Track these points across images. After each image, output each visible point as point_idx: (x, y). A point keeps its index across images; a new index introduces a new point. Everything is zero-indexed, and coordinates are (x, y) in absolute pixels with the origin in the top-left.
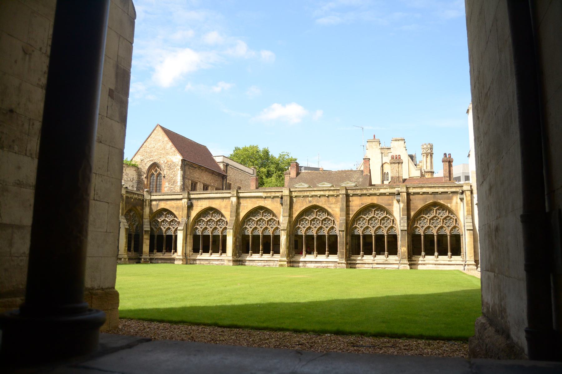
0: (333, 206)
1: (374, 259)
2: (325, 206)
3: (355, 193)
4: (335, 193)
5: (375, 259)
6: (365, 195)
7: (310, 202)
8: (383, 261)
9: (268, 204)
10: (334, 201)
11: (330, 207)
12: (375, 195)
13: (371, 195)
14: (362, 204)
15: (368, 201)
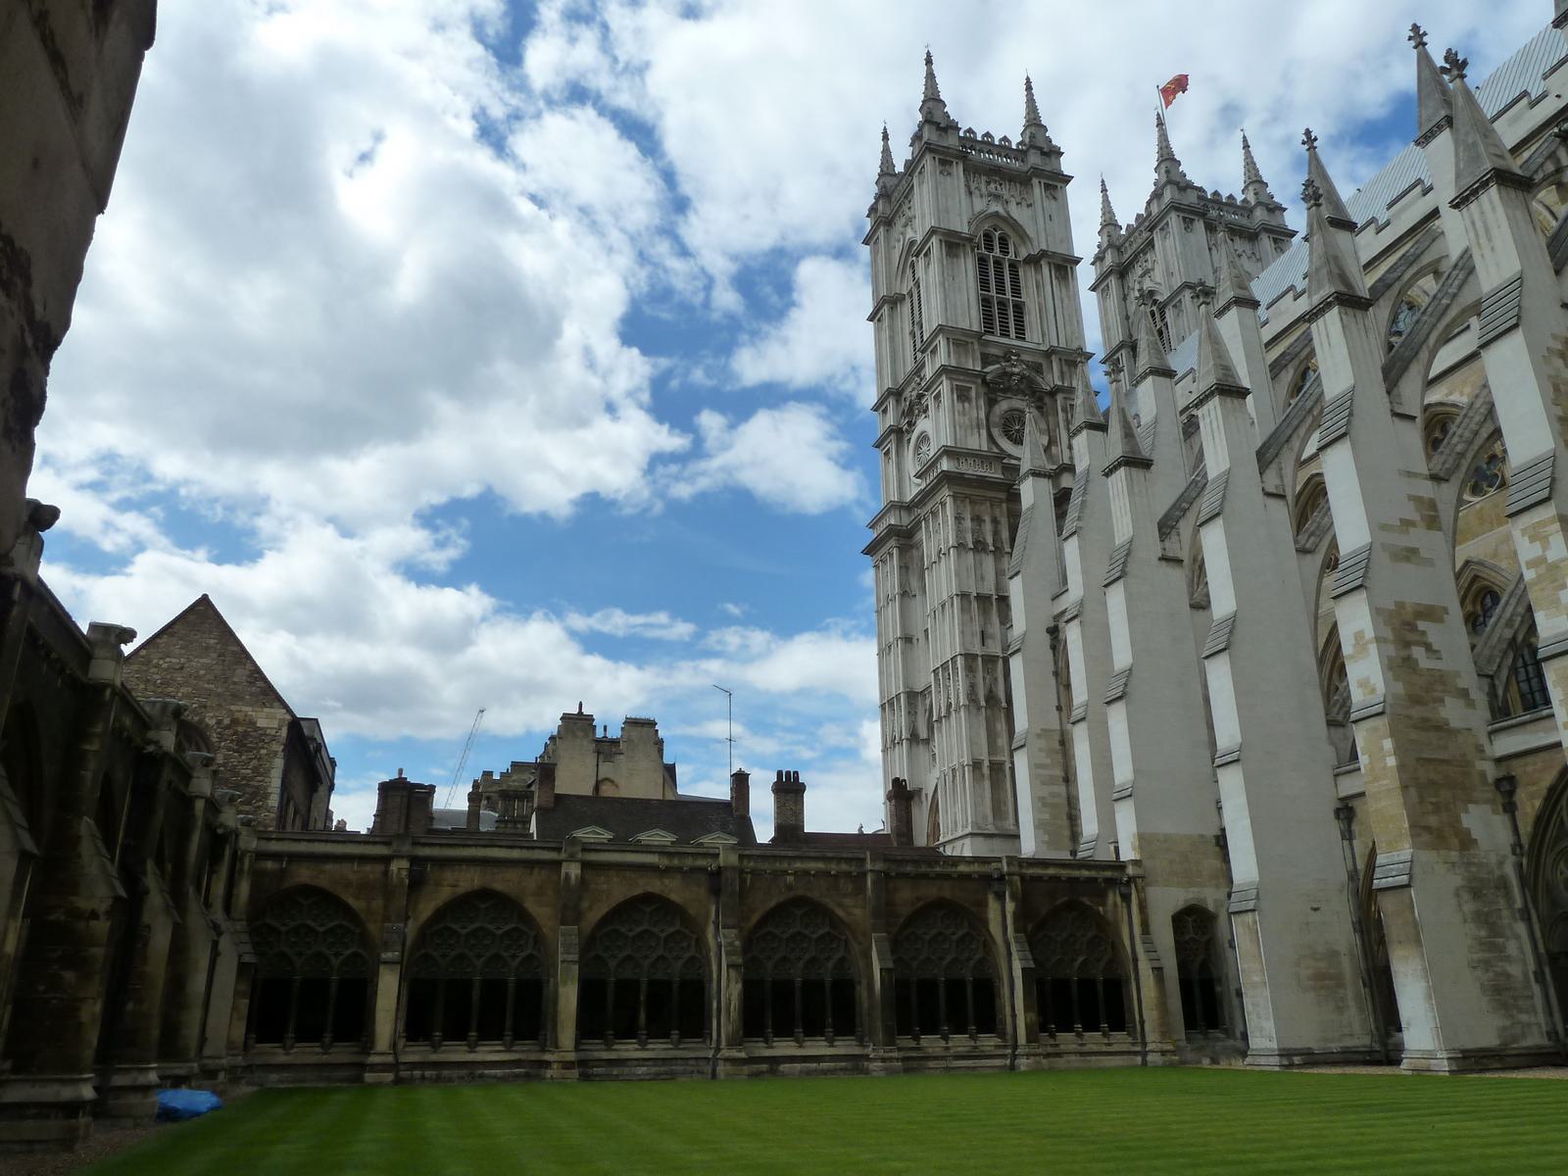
0: (848, 901)
1: (947, 1043)
2: (828, 900)
3: (902, 870)
4: (853, 869)
5: (950, 1044)
6: (925, 876)
7: (790, 888)
8: (967, 1049)
9: (673, 889)
10: (850, 890)
11: (841, 905)
12: (947, 877)
13: (940, 876)
14: (918, 899)
15: (931, 891)
